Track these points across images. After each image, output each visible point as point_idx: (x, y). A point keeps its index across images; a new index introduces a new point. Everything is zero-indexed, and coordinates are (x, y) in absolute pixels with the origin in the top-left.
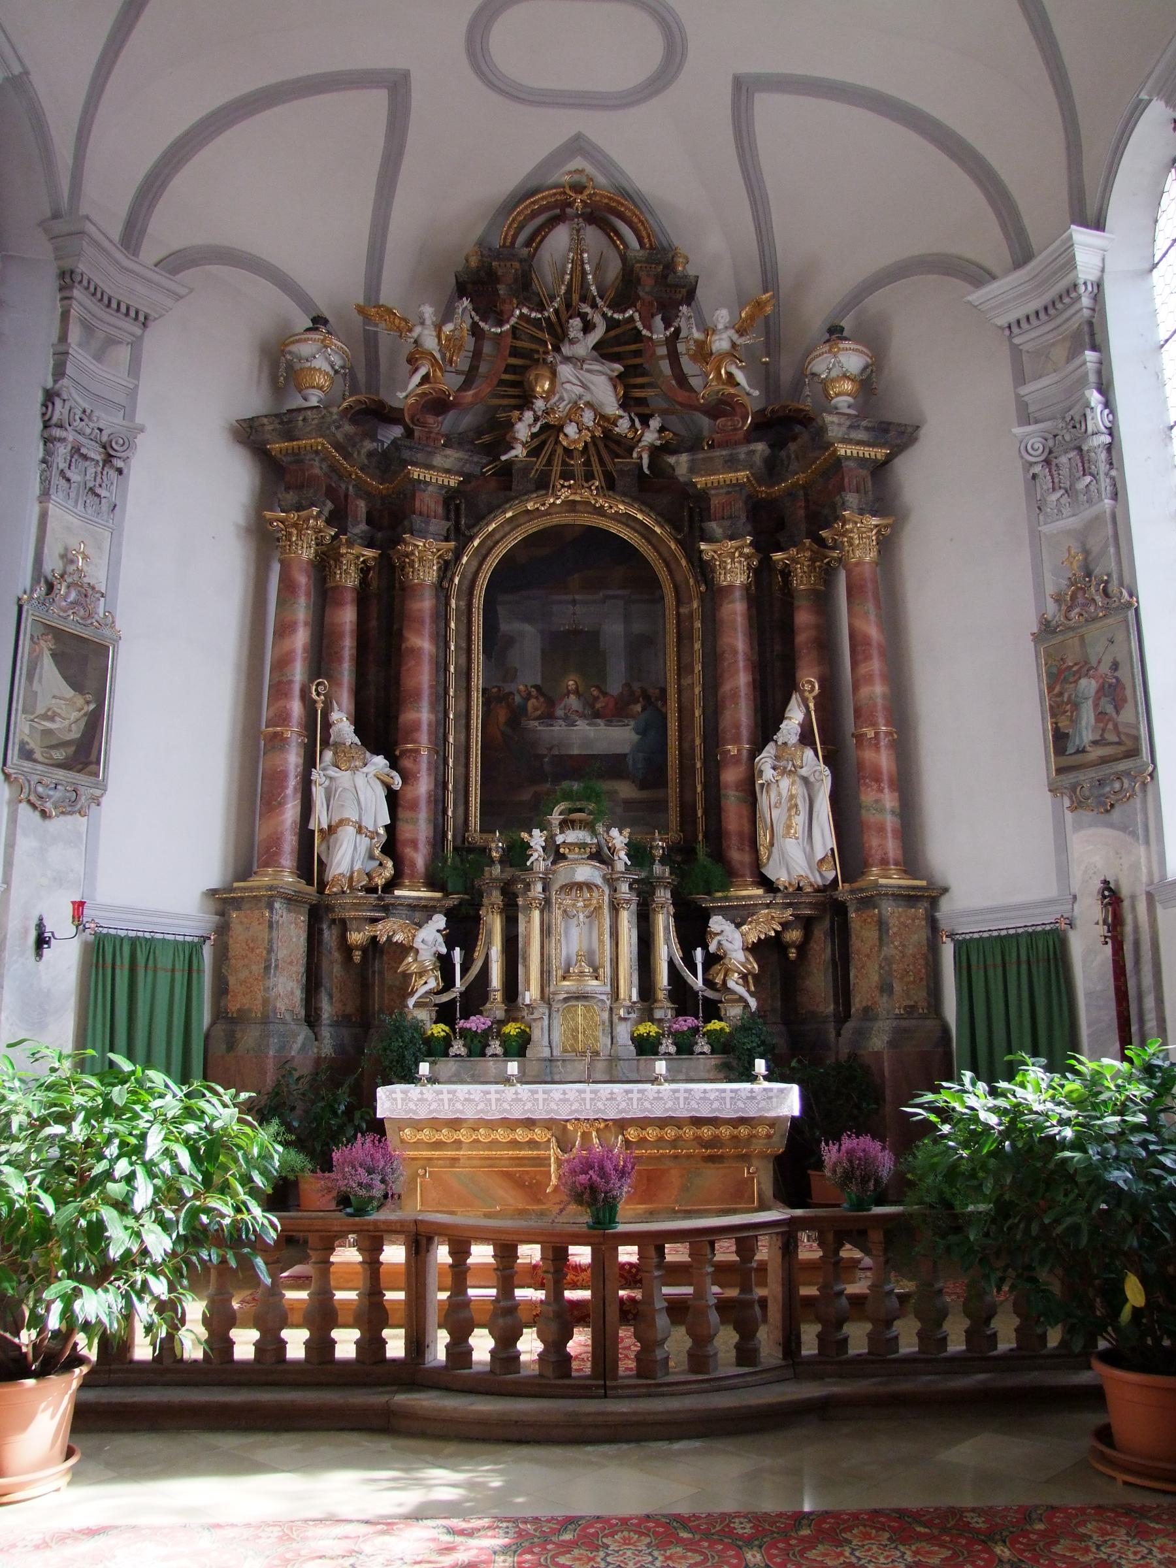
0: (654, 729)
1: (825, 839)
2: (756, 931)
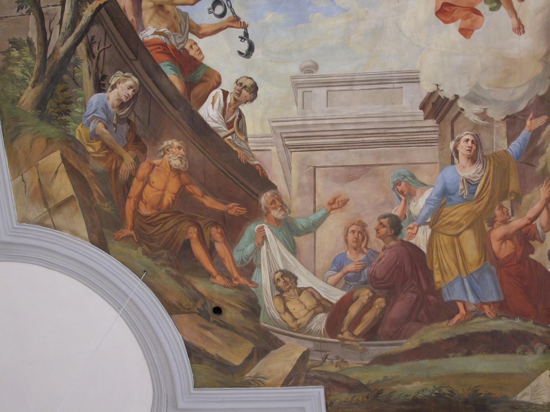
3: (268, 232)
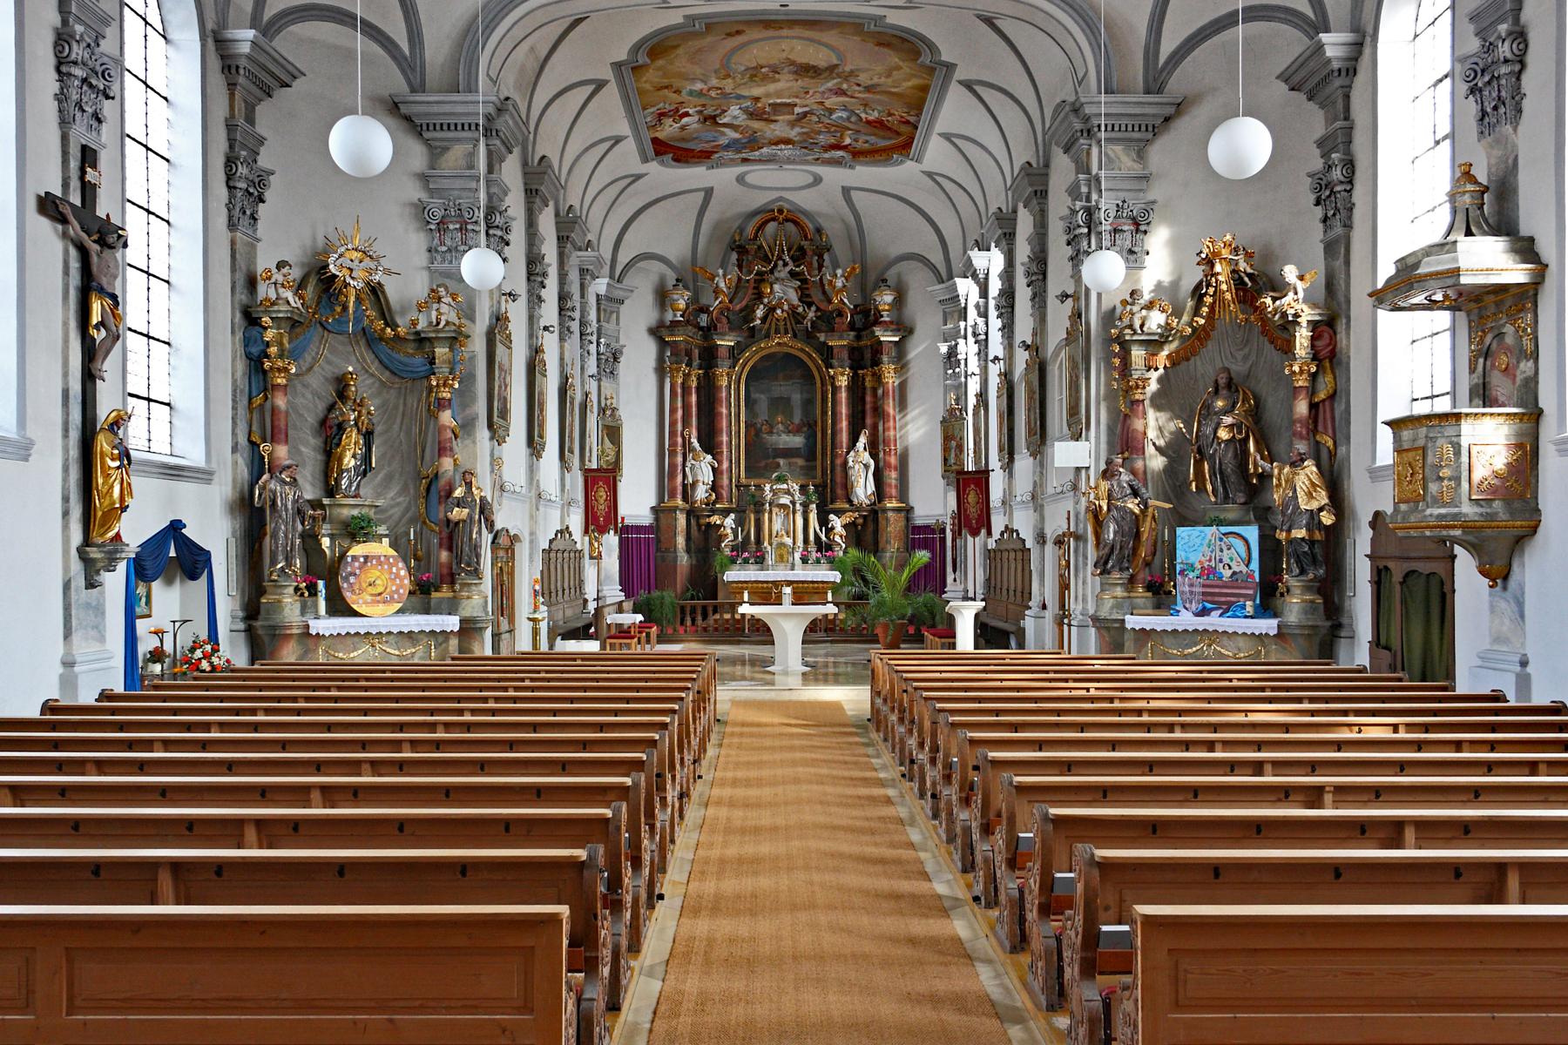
0: (811, 437)
1: (871, 488)
2: (847, 518)
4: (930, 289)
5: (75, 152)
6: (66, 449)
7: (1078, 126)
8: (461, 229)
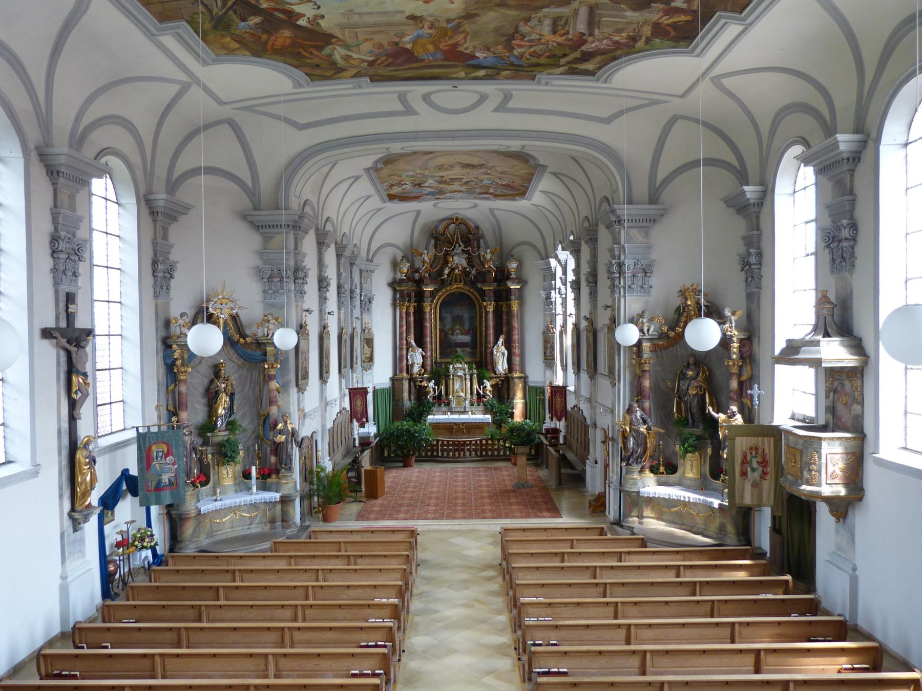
1: (506, 366)
3: (336, 47)
4: (536, 262)
5: (63, 298)
6: (60, 462)
7: (613, 219)
8: (280, 280)
